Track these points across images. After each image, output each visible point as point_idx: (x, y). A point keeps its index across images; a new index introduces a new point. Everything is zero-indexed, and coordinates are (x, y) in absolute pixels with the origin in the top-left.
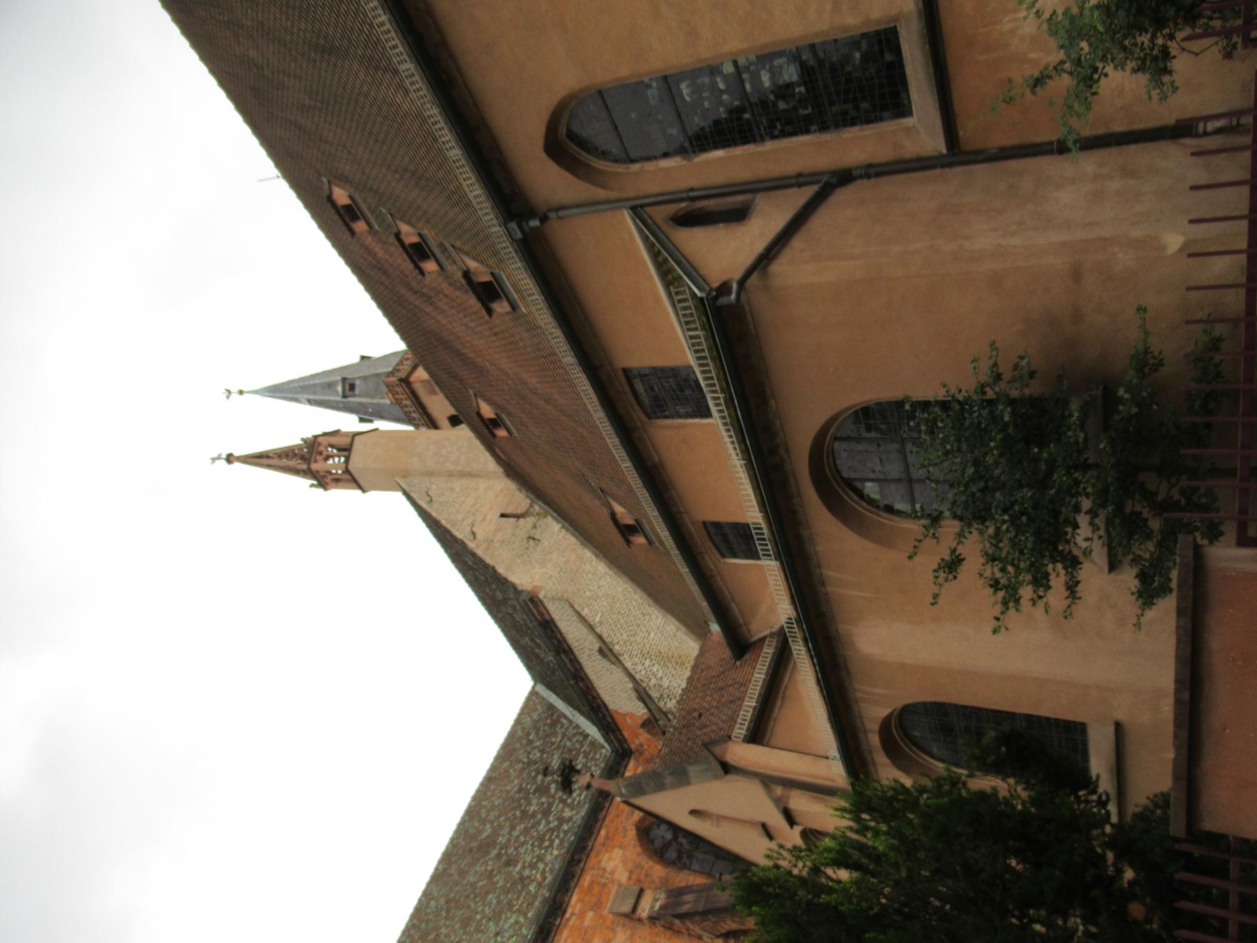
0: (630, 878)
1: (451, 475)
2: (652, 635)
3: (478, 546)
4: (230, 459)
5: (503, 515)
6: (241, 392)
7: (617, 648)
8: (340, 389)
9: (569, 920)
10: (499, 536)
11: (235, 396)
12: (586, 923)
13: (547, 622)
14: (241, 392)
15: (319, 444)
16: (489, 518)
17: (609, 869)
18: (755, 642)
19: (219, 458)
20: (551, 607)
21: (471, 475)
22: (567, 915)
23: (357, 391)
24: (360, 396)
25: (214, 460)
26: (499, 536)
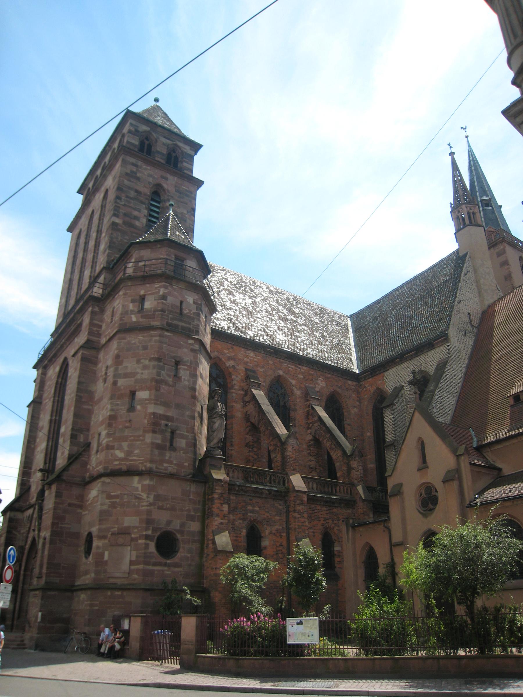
0: (318, 392)
1: (477, 282)
2: (448, 400)
3: (456, 306)
4: (452, 154)
5: (469, 314)
6: (467, 137)
7: (440, 385)
8: (485, 198)
9: (298, 367)
10: (462, 315)
11: (463, 133)
12: (299, 376)
13: (433, 346)
14: (467, 137)
15: (475, 207)
16: (467, 307)
17: (318, 381)
18: (482, 454)
19: (451, 147)
20: (442, 348)
21: (480, 293)
22: (299, 366)
23: (485, 208)
24: (483, 210)
25: (449, 144)
26: (462, 315)
